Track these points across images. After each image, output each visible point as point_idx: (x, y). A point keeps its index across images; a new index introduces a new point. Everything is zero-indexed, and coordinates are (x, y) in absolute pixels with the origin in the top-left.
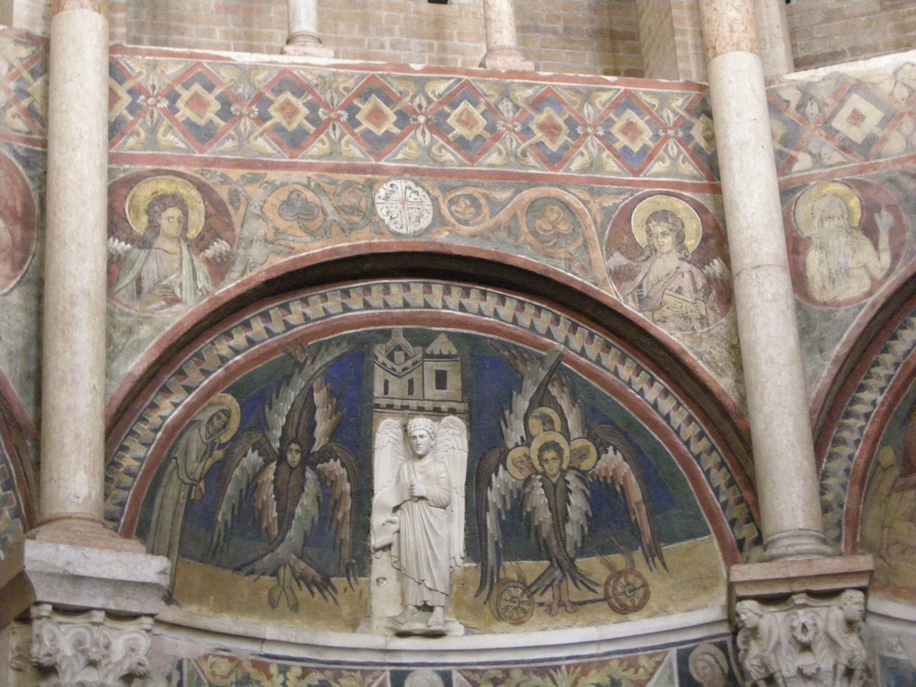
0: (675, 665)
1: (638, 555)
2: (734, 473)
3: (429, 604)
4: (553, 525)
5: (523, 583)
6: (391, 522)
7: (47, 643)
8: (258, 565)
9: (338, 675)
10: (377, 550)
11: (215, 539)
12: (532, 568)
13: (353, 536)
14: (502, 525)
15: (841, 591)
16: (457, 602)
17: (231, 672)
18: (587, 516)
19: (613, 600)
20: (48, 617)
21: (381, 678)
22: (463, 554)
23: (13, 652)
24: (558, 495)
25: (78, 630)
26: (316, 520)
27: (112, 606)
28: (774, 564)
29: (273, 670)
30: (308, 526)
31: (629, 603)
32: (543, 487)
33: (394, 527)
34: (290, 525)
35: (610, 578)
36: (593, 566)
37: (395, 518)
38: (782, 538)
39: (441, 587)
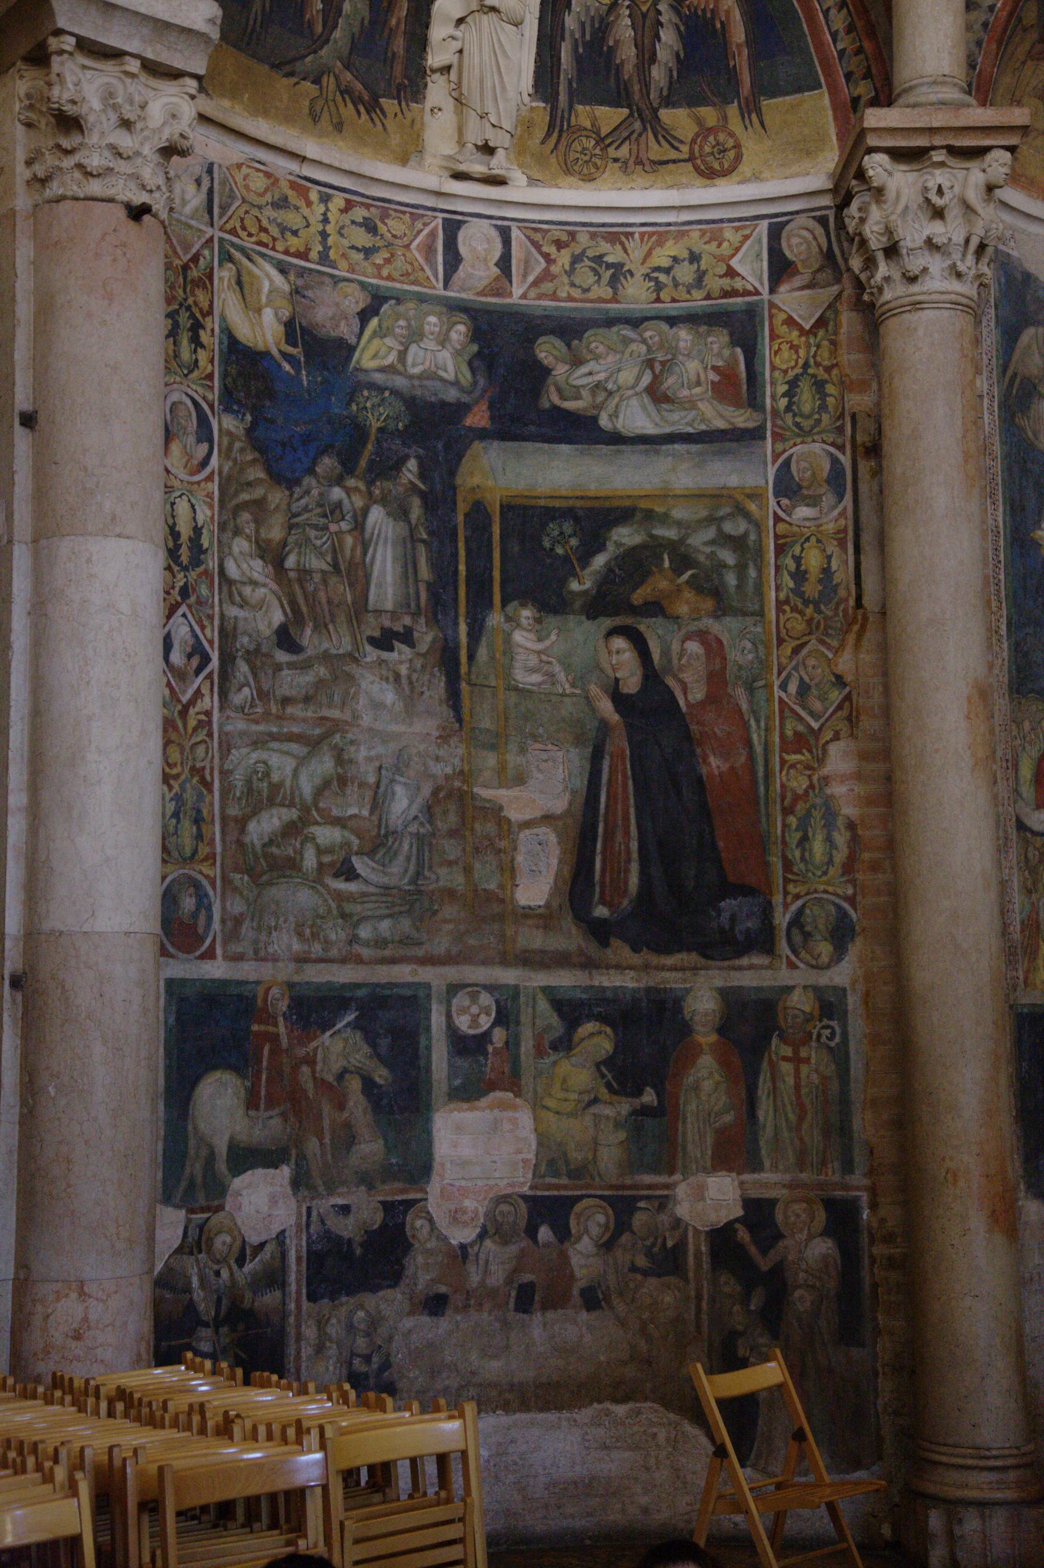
0: (765, 240)
1: (733, 110)
2: (855, 18)
3: (491, 144)
4: (637, 66)
5: (598, 134)
6: (453, 38)
7: (70, 86)
8: (299, 66)
9: (384, 216)
10: (434, 71)
11: (251, 22)
12: (609, 116)
13: (407, 50)
14: (578, 59)
15: (988, 149)
16: (520, 150)
17: (266, 190)
18: (677, 55)
19: (699, 162)
20: (71, 54)
21: (433, 225)
22: (531, 91)
23: (21, 101)
24: (647, 28)
25: (106, 80)
26: (366, 22)
27: (149, 55)
28: (916, 111)
29: (314, 196)
30: (356, 30)
31: (717, 166)
32: (630, 16)
33: (456, 45)
34: (335, 26)
35: (697, 135)
36: (678, 119)
37: (458, 34)
38: (922, 84)
39: (507, 125)
